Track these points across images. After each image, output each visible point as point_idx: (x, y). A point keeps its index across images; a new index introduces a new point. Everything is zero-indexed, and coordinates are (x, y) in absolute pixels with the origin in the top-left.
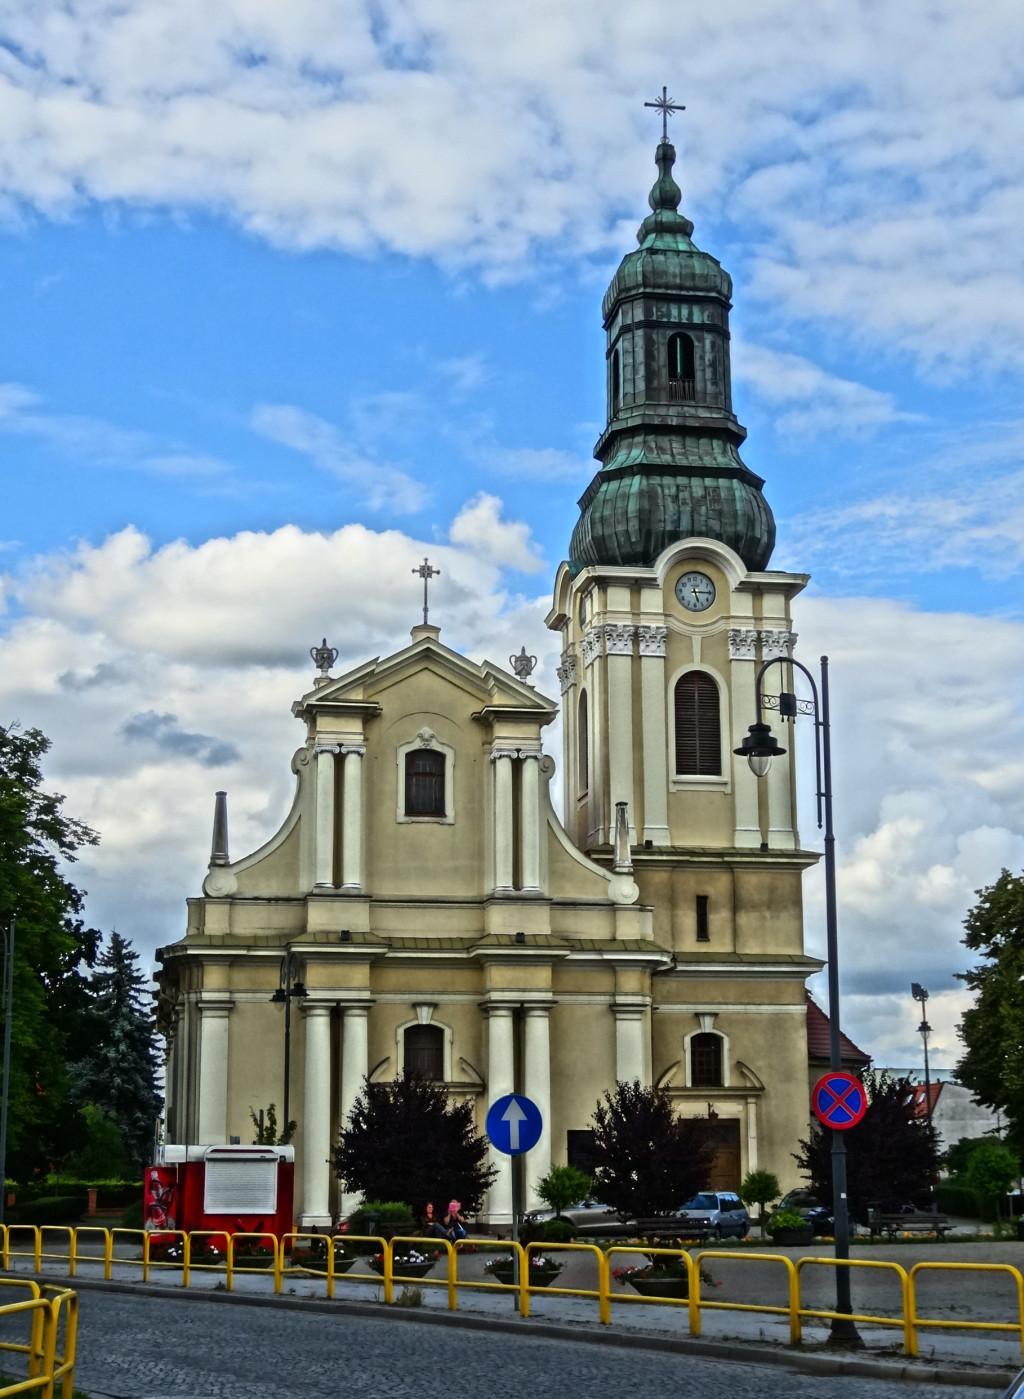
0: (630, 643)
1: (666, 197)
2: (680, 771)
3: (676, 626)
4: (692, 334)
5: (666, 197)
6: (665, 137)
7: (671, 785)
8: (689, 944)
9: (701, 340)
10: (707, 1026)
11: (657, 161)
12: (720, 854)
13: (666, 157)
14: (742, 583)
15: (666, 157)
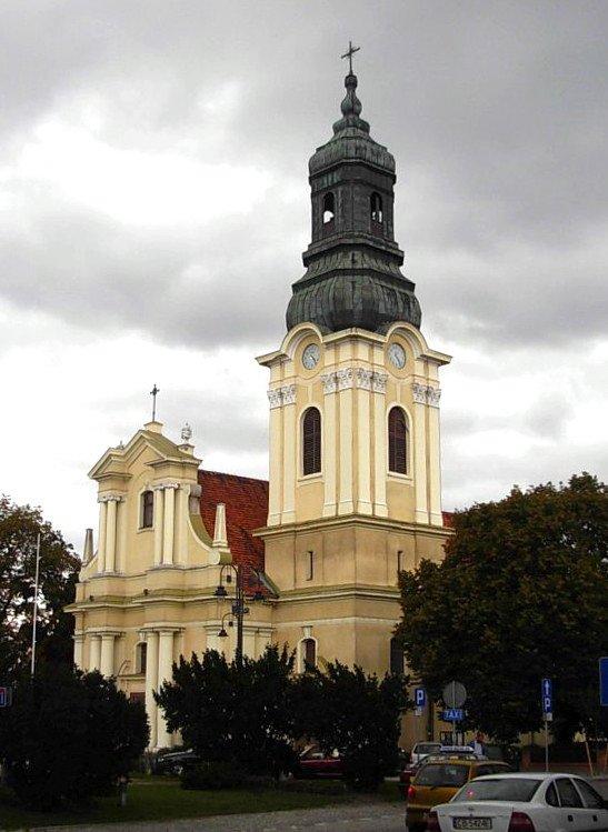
0: (279, 400)
1: (351, 108)
2: (306, 474)
3: (300, 381)
4: (333, 191)
5: (351, 108)
6: (351, 71)
7: (298, 485)
8: (303, 584)
9: (337, 193)
10: (307, 636)
11: (346, 85)
12: (307, 523)
13: (351, 82)
14: (327, 344)
15: (351, 82)
